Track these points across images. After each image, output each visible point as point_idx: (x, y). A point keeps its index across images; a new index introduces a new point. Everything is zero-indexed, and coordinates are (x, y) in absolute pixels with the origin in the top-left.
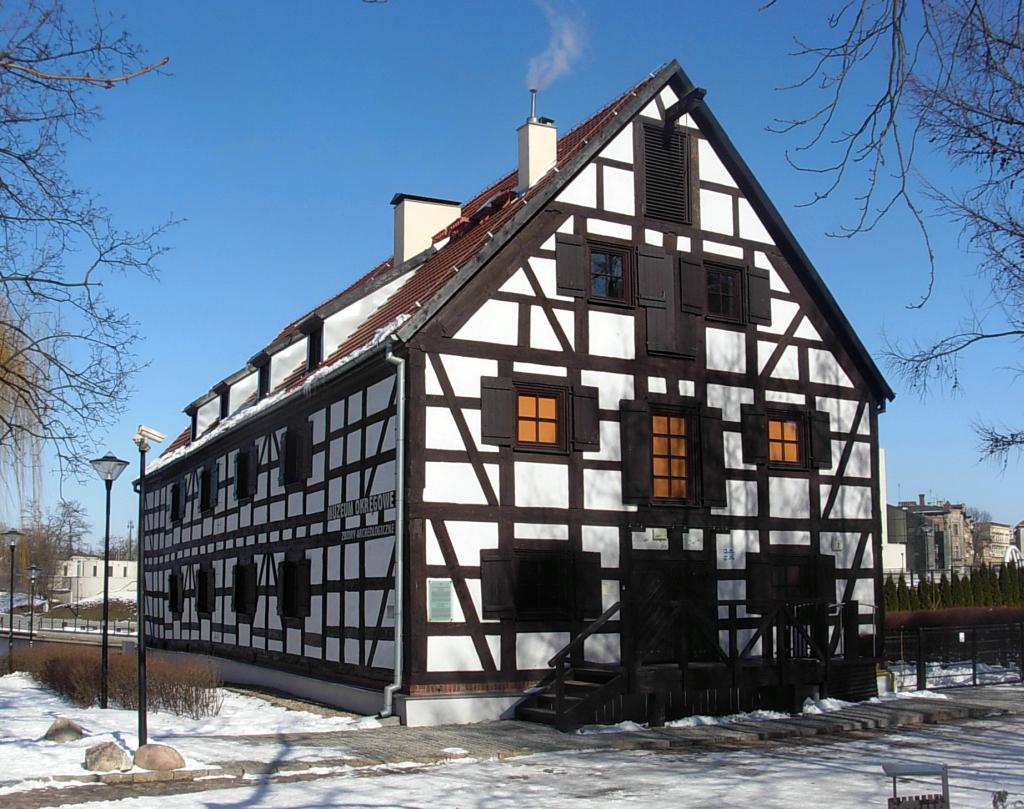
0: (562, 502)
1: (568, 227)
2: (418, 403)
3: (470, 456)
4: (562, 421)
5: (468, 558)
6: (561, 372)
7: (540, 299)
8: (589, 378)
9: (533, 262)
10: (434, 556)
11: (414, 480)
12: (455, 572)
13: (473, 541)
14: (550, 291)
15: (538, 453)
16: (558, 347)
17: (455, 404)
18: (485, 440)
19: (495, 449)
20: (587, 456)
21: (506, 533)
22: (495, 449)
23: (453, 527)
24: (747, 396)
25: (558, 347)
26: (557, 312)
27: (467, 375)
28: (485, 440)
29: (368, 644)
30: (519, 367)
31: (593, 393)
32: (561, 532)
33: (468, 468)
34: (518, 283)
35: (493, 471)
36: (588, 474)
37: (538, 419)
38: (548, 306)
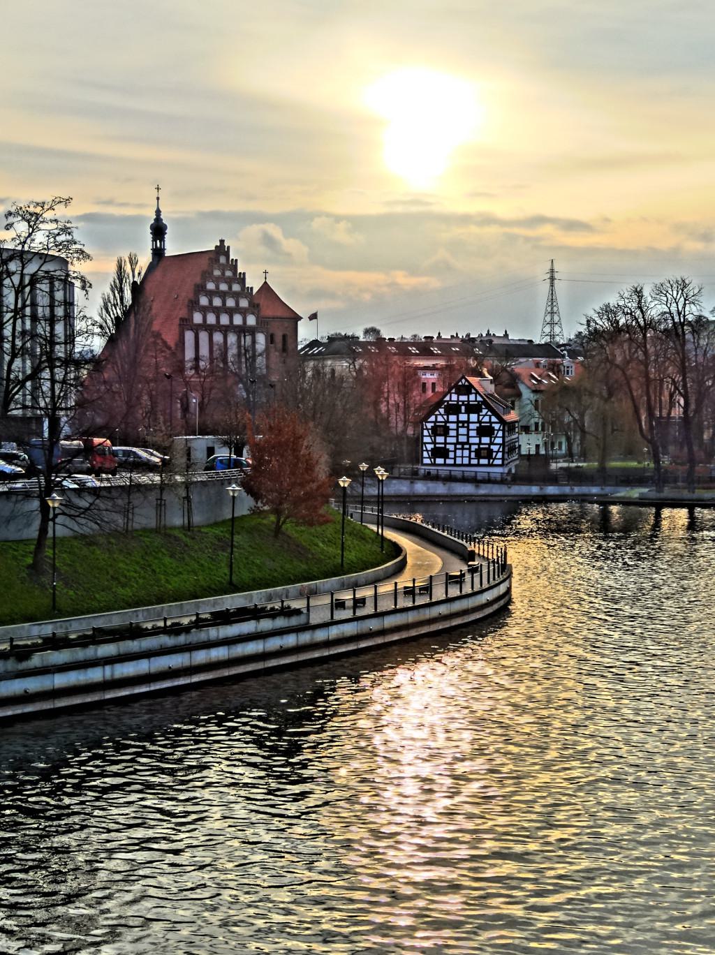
2: (423, 429)
3: (429, 436)
4: (444, 431)
7: (440, 414)
8: (448, 425)
11: (422, 439)
12: (427, 450)
13: (430, 447)
14: (443, 413)
15: (440, 435)
17: (427, 429)
24: (478, 425)
27: (429, 426)
32: (443, 446)
34: (437, 413)
36: (448, 438)
37: (440, 431)
38: (442, 415)
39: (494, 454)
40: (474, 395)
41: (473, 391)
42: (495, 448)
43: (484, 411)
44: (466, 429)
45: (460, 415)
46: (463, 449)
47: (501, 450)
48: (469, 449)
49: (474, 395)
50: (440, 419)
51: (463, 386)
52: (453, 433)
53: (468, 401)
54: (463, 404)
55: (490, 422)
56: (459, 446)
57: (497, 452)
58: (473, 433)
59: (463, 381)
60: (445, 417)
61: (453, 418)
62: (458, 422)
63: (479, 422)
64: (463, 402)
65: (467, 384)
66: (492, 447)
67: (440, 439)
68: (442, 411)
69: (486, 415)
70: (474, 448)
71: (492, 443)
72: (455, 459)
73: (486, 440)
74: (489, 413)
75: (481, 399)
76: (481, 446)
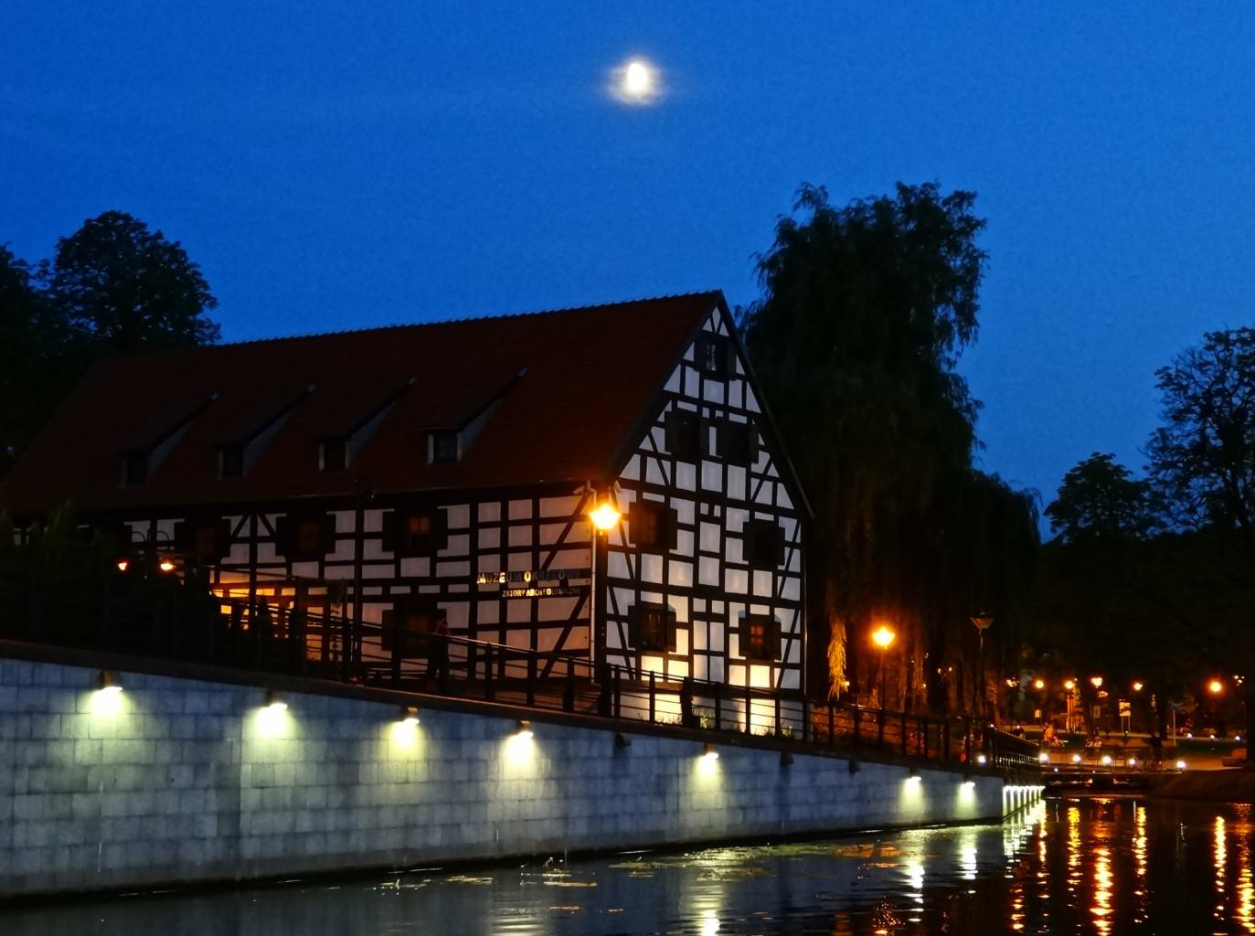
0: (659, 580)
1: (669, 408)
3: (623, 549)
5: (623, 611)
6: (661, 499)
7: (655, 454)
9: (654, 430)
10: (610, 610)
12: (617, 618)
13: (625, 598)
14: (661, 449)
16: (663, 483)
18: (631, 542)
19: (634, 546)
20: (671, 551)
21: (638, 596)
22: (634, 546)
23: (616, 590)
25: (663, 483)
26: (663, 462)
28: (631, 542)
29: (542, 664)
30: (646, 496)
31: (675, 512)
33: (623, 555)
34: (646, 445)
35: (633, 557)
36: (672, 563)
38: (659, 457)
39: (784, 642)
40: (739, 383)
41: (740, 370)
42: (784, 617)
43: (764, 457)
44: (718, 527)
45: (705, 463)
46: (708, 617)
47: (797, 631)
48: (724, 618)
49: (739, 383)
50: (654, 476)
51: (714, 337)
52: (684, 542)
53: (726, 408)
54: (713, 421)
55: (773, 509)
56: (700, 605)
57: (790, 636)
58: (735, 551)
59: (716, 315)
60: (667, 465)
61: (685, 476)
62: (699, 495)
63: (749, 504)
64: (713, 406)
65: (724, 332)
66: (779, 612)
67: (653, 568)
68: (659, 434)
69: (763, 477)
70: (736, 609)
71: (775, 601)
72: (689, 659)
73: (763, 583)
74: (773, 472)
75: (757, 410)
76: (756, 609)
